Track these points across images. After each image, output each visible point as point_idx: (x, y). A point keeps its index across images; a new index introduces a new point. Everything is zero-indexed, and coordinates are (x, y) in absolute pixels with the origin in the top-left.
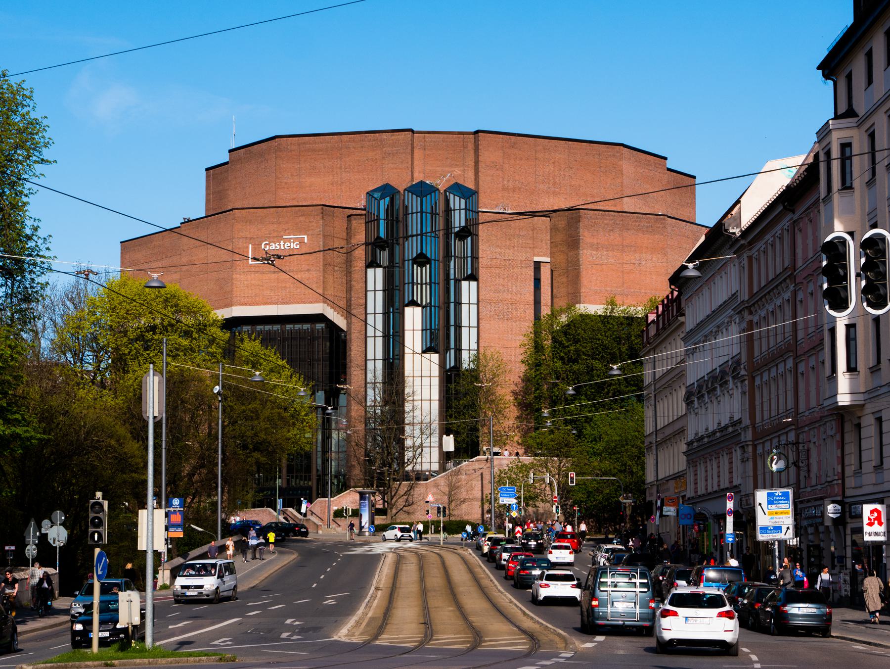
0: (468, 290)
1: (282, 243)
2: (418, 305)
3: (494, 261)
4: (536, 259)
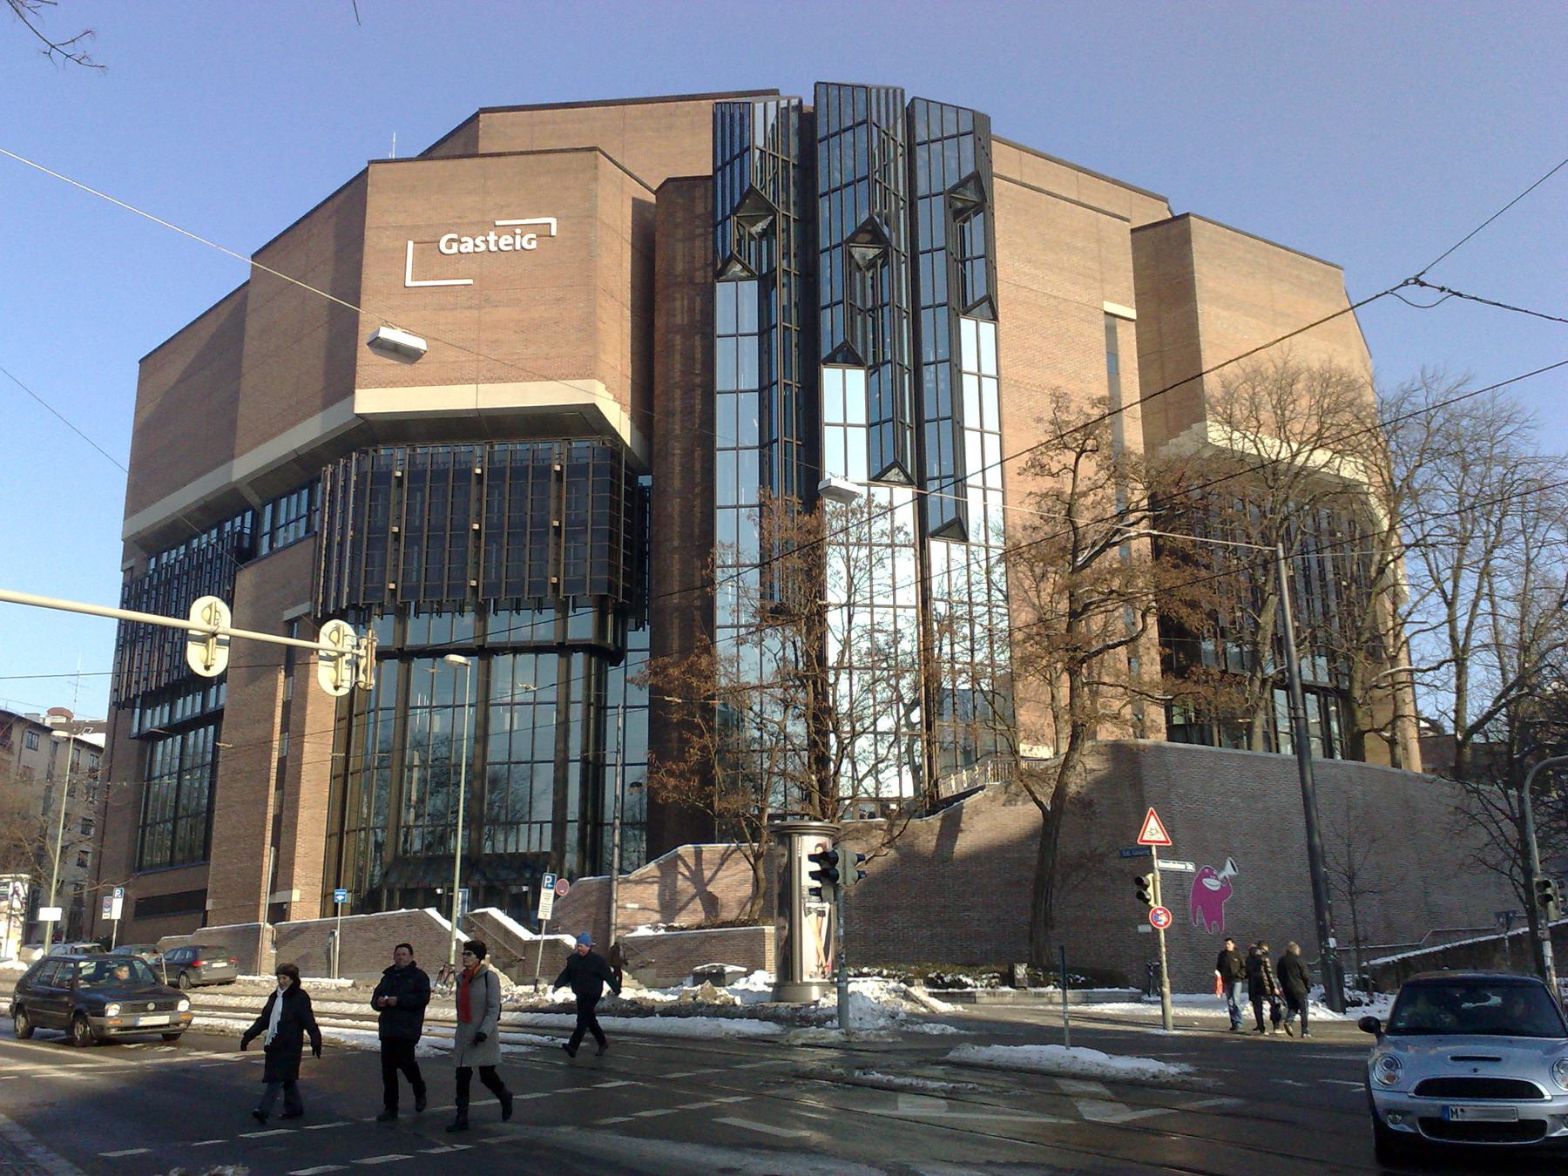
1: (492, 237)
2: (857, 363)
3: (1024, 292)
4: (1110, 307)
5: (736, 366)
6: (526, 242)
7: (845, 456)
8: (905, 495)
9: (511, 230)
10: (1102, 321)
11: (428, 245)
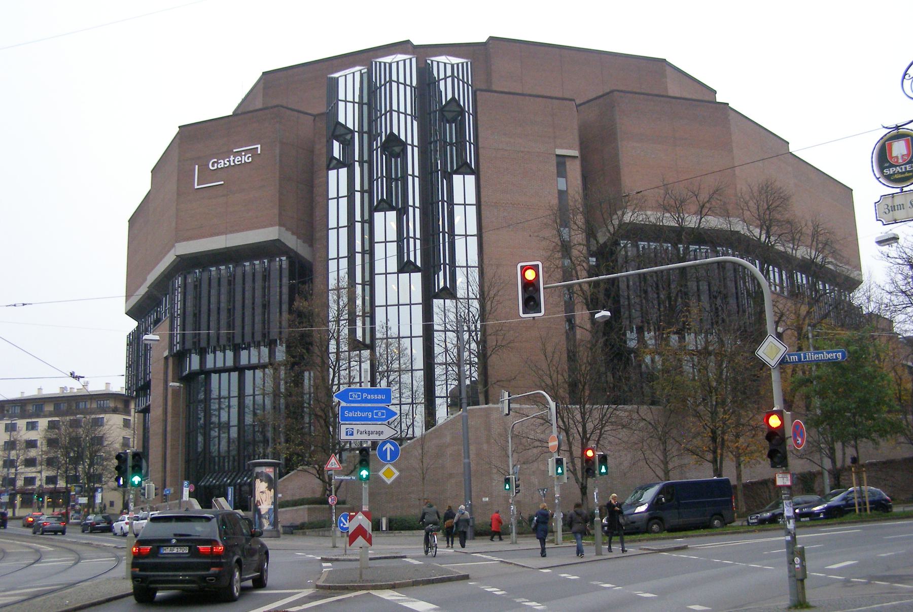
0: (464, 187)
1: (232, 158)
2: (392, 208)
4: (559, 152)
5: (337, 213)
6: (246, 159)
7: (386, 257)
8: (417, 277)
9: (239, 153)
10: (554, 161)
11: (204, 168)
